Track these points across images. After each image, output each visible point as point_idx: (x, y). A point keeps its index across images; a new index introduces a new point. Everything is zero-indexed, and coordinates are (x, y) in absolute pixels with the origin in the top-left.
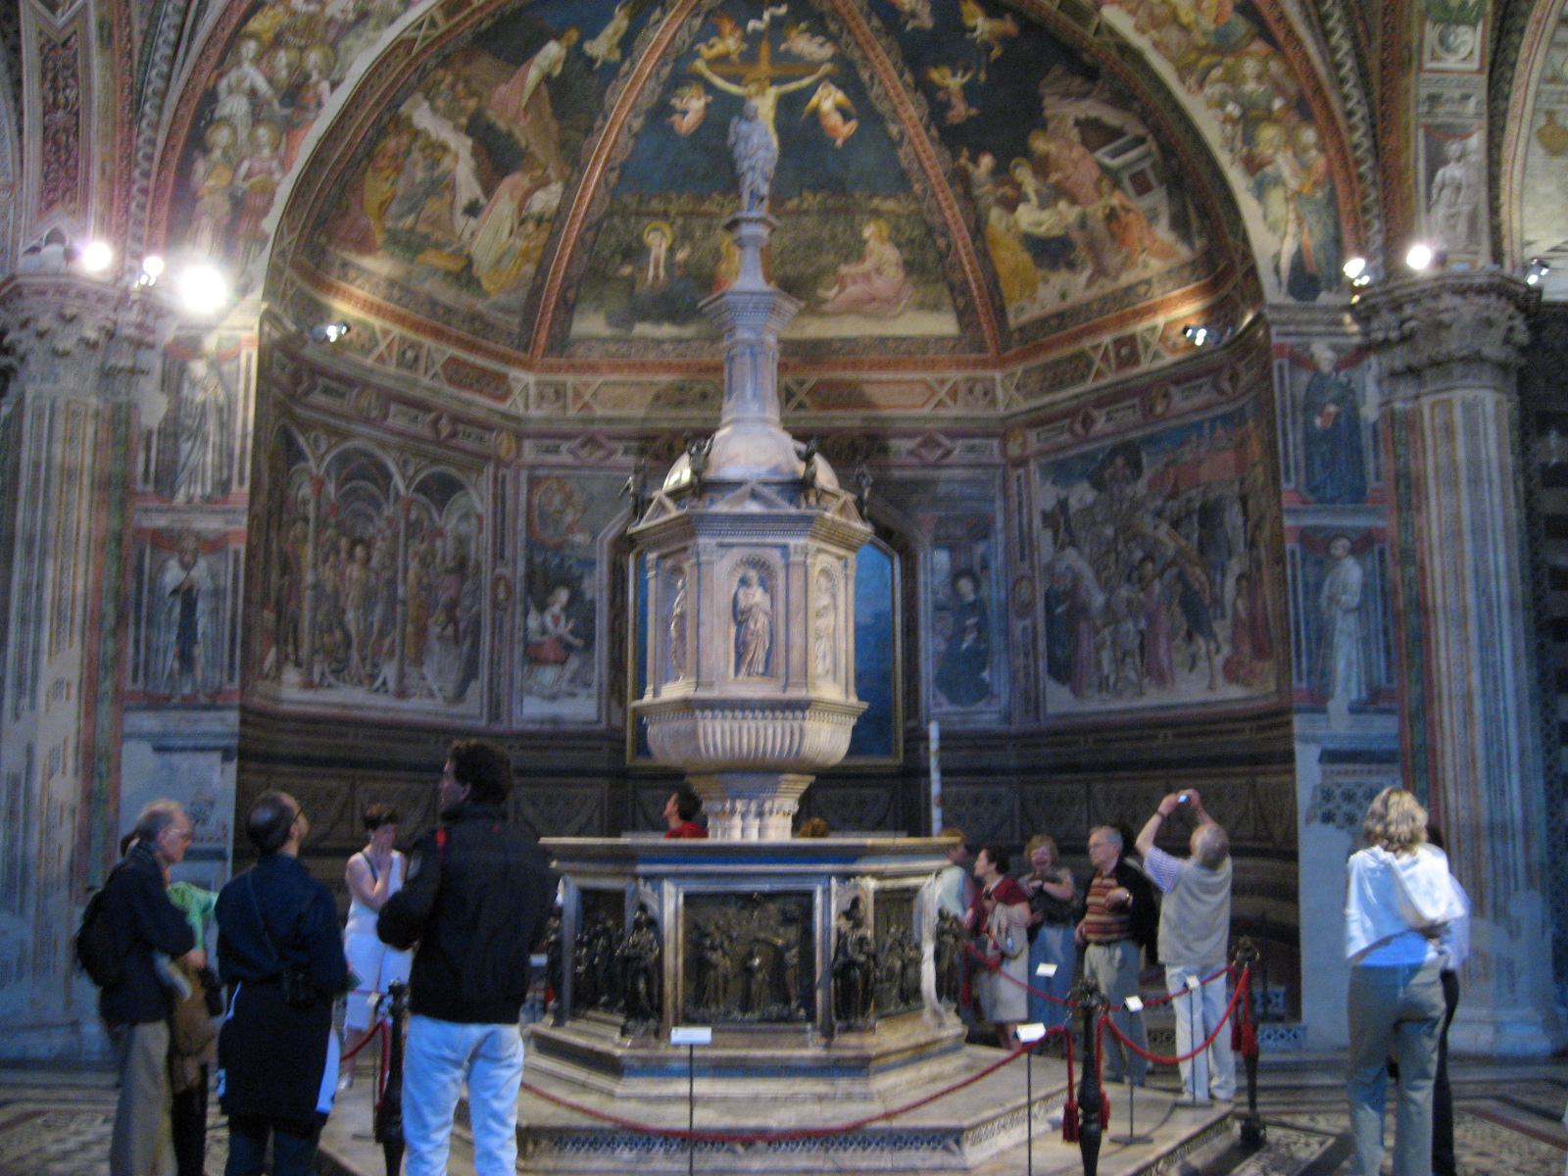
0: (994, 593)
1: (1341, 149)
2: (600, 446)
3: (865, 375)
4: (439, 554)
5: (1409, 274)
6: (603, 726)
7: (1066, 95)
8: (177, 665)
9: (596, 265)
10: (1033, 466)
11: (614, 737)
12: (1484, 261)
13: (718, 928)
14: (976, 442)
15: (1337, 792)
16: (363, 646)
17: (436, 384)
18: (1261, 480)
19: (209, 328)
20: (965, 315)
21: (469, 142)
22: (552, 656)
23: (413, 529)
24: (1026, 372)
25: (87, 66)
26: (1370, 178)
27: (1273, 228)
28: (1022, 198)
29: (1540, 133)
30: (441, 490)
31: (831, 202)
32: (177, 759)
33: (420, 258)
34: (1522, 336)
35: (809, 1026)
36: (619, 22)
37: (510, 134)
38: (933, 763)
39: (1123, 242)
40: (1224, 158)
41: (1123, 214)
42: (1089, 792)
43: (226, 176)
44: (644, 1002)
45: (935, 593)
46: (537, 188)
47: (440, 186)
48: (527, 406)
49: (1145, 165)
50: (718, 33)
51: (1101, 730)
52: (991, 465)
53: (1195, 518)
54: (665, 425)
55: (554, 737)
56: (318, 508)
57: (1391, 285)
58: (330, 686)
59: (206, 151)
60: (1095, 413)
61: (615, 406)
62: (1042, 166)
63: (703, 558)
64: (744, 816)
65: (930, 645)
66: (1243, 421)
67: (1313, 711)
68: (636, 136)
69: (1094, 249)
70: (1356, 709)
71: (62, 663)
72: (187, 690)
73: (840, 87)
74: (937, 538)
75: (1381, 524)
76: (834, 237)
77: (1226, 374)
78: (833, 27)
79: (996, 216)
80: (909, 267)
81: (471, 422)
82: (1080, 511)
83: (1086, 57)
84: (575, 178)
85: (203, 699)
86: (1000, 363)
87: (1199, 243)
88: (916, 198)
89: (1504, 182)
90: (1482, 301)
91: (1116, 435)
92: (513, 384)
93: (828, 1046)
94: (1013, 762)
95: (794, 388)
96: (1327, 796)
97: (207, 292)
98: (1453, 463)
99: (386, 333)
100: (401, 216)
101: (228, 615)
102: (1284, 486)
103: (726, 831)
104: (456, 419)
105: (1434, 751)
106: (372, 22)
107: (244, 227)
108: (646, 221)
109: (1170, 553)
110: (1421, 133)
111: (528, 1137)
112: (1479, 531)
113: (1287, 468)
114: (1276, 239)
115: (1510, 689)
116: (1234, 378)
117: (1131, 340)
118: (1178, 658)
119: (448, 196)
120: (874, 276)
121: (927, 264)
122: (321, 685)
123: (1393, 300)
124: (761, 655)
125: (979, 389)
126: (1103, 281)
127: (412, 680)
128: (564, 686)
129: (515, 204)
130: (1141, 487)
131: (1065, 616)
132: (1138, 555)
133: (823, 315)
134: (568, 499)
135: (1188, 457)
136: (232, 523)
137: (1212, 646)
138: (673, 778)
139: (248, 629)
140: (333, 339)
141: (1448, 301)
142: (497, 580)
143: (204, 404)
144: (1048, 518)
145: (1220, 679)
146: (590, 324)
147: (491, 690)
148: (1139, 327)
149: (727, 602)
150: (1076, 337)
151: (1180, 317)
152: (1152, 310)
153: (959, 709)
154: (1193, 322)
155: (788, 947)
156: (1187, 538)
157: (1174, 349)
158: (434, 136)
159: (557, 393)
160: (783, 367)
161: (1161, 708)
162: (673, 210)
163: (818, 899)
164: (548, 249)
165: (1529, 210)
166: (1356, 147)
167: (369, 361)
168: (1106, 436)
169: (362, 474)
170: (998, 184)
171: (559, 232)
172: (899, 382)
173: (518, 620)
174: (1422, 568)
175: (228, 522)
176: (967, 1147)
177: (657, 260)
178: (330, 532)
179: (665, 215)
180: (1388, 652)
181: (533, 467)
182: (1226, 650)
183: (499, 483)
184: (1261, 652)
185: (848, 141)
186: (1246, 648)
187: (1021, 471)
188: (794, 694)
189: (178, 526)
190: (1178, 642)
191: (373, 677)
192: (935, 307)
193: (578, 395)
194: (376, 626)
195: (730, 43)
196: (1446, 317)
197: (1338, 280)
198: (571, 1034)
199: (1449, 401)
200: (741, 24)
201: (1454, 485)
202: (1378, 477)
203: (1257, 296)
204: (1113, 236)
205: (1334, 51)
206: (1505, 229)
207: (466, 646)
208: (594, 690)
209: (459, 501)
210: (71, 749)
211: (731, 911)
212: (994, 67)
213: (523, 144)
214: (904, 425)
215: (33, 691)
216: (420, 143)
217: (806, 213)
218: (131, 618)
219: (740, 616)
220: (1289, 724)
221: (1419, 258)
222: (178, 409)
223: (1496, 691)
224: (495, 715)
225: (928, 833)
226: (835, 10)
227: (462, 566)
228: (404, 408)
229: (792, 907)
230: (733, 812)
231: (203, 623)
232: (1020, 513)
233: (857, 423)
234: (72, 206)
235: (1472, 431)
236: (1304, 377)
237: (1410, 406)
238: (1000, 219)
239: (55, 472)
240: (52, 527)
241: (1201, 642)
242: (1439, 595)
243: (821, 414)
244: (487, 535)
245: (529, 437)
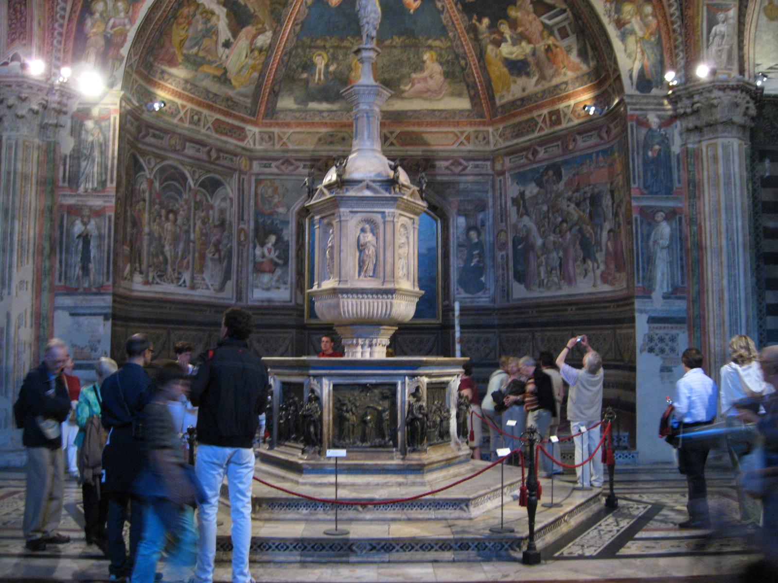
0: (488, 238)
1: (664, 16)
2: (292, 164)
3: (423, 129)
4: (211, 219)
5: (697, 80)
6: (293, 303)
8: (81, 273)
9: (290, 73)
10: (507, 175)
11: (299, 309)
12: (735, 73)
13: (350, 401)
14: (478, 163)
15: (656, 337)
16: (174, 263)
17: (209, 133)
18: (621, 183)
19: (95, 104)
20: (473, 99)
21: (225, 10)
22: (268, 269)
23: (198, 205)
24: (504, 128)
26: (679, 30)
27: (629, 56)
28: (504, 40)
29: (765, 9)
30: (212, 186)
31: (407, 42)
32: (81, 319)
33: (201, 69)
34: (753, 112)
35: (394, 449)
37: (246, 6)
38: (457, 322)
39: (554, 63)
40: (605, 20)
41: (553, 48)
42: (533, 338)
43: (102, 27)
44: (313, 437)
45: (458, 238)
46: (259, 34)
47: (211, 32)
48: (255, 144)
49: (566, 23)
51: (539, 306)
52: (487, 175)
53: (588, 202)
54: (324, 154)
55: (268, 309)
56: (151, 194)
57: (688, 85)
58: (157, 283)
59: (92, 14)
60: (539, 149)
61: (298, 145)
62: (514, 24)
63: (343, 218)
64: (362, 346)
65: (455, 263)
66: (612, 153)
67: (645, 297)
68: (309, 8)
69: (538, 65)
70: (666, 297)
71: (23, 272)
72: (86, 285)
74: (459, 210)
75: (680, 205)
76: (409, 59)
77: (604, 130)
79: (490, 48)
80: (447, 75)
81: (227, 152)
82: (531, 198)
84: (278, 28)
85: (94, 290)
86: (492, 123)
87: (592, 64)
88: (450, 40)
89: (746, 34)
90: (733, 93)
91: (549, 160)
92: (248, 133)
93: (403, 459)
94: (496, 322)
95: (389, 135)
96: (651, 339)
97: (93, 86)
98: (717, 175)
99: (184, 107)
100: (192, 47)
101: (106, 248)
102: (633, 186)
103: (354, 353)
104: (219, 150)
105: (704, 317)
107: (111, 53)
108: (314, 50)
109: (576, 218)
110: (705, 8)
111: (257, 502)
112: (728, 208)
113: (634, 178)
114: (631, 61)
115: (742, 287)
116: (608, 132)
117: (557, 112)
118: (578, 271)
119: (214, 38)
120: (428, 79)
121: (456, 73)
122: (153, 283)
123: (689, 93)
124: (371, 267)
125: (481, 136)
126: (544, 82)
127: (198, 281)
128: (273, 283)
129: (248, 42)
130: (561, 186)
131: (523, 249)
132: (559, 219)
133: (403, 98)
134: (275, 190)
135: (585, 171)
136: (108, 202)
137: (596, 265)
138: (328, 329)
139: (116, 255)
140: (157, 109)
141: (716, 93)
142: (240, 231)
143: (92, 143)
144: (515, 201)
145: (599, 282)
146: (286, 103)
147: (237, 286)
148: (561, 106)
149: (354, 241)
150: (530, 110)
151: (582, 100)
152: (568, 97)
153: (469, 296)
154: (588, 103)
155: (384, 411)
156: (584, 211)
157: (579, 117)
158: (207, 7)
159: (270, 137)
160: (382, 125)
161: (570, 295)
162: (328, 45)
163: (399, 388)
164: (265, 64)
165: (758, 48)
166: (672, 15)
167: (175, 121)
168: (544, 160)
169: (173, 178)
170: (491, 34)
171: (271, 56)
172: (441, 133)
173: (251, 250)
174: (700, 227)
175: (105, 202)
176: (472, 508)
177: (320, 70)
178: (157, 207)
179: (324, 47)
180: (682, 267)
181: (258, 174)
182: (602, 267)
183: (241, 182)
184: (619, 269)
185: (416, 10)
186: (612, 267)
187: (501, 178)
188: (388, 286)
189: (80, 203)
190: (579, 263)
191: (179, 279)
192: (460, 95)
193: (280, 138)
196: (715, 102)
197: (661, 82)
198: (278, 453)
199: (716, 144)
201: (717, 186)
202: (679, 181)
203: (621, 90)
204: (549, 60)
206: (746, 57)
208: (289, 285)
209: (220, 192)
210: (29, 315)
211: (356, 393)
213: (252, 11)
214: (444, 154)
215: (10, 285)
216: (200, 10)
217: (395, 47)
218: (58, 249)
219: (361, 247)
220: (633, 303)
221: (702, 71)
222: (80, 145)
223: (735, 288)
224: (239, 298)
225: (454, 356)
227: (223, 224)
228: (192, 145)
229: (386, 391)
230: (357, 344)
231: (93, 252)
232: (501, 199)
233: (420, 153)
234: (24, 42)
235: (727, 159)
236: (644, 131)
237: (696, 146)
238: (492, 50)
239: (18, 176)
240: (17, 204)
241: (590, 263)
242: (709, 241)
243: (402, 148)
244: (235, 208)
245: (256, 159)
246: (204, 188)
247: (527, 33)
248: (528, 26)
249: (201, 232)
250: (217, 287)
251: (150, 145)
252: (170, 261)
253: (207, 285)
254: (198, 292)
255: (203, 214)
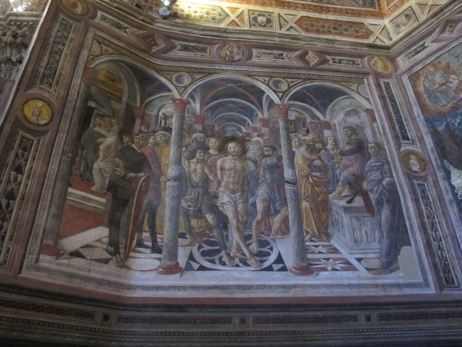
4: (330, 142)
16: (244, 225)
56: (182, 119)
58: (202, 268)
104: (321, 53)
122: (189, 268)
127: (318, 251)
134: (448, 70)
159: (407, 16)
173: (443, 184)
194: (260, 207)
207: (385, 213)
209: (342, 103)
227: (359, 148)
245: (400, 54)
246: (304, 102)
249: (310, 166)
250: (375, 264)
251: (181, 60)
252: (233, 222)
253: (348, 263)
254: (323, 278)
255: (310, 137)
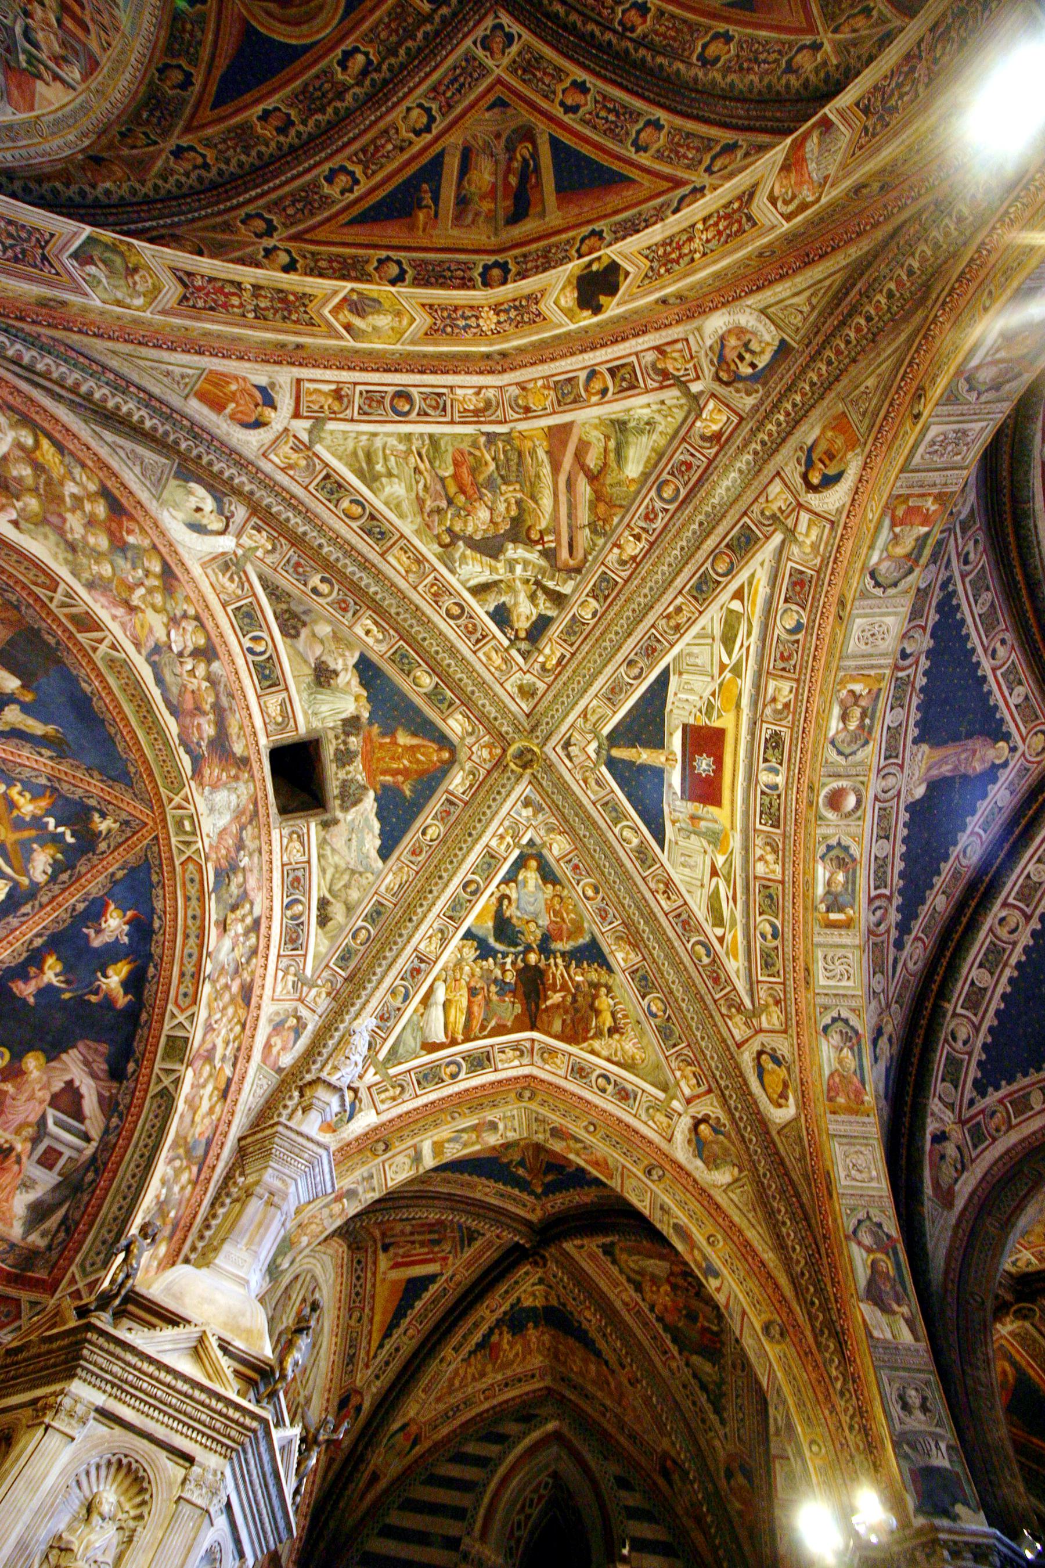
7: (86, 1063)
25: (30, 279)
36: (37, 728)
49: (67, 1153)
50: (33, 799)
73: (10, 895)
78: (64, 877)
83: (131, 1067)
87: (36, 1239)
106: (70, 557)
195: (27, 808)
200: (48, 813)
205: (214, 1216)
212: (80, 1001)
226: (80, 876)
247: (8, 1101)
248: (23, 1097)
